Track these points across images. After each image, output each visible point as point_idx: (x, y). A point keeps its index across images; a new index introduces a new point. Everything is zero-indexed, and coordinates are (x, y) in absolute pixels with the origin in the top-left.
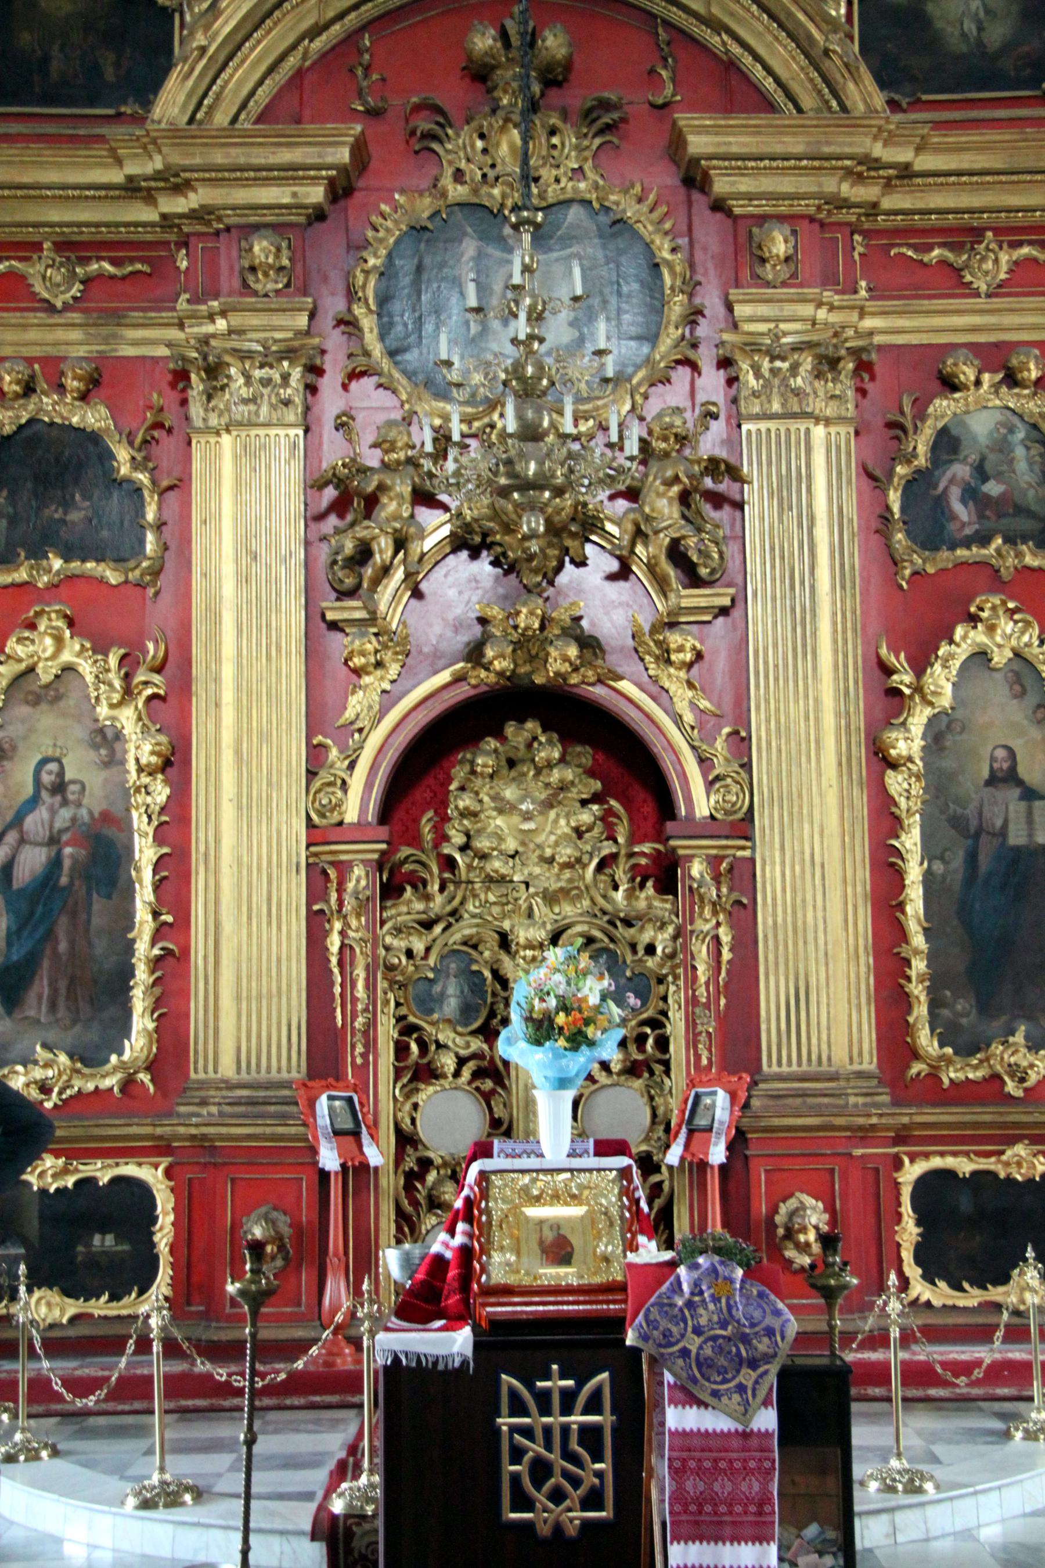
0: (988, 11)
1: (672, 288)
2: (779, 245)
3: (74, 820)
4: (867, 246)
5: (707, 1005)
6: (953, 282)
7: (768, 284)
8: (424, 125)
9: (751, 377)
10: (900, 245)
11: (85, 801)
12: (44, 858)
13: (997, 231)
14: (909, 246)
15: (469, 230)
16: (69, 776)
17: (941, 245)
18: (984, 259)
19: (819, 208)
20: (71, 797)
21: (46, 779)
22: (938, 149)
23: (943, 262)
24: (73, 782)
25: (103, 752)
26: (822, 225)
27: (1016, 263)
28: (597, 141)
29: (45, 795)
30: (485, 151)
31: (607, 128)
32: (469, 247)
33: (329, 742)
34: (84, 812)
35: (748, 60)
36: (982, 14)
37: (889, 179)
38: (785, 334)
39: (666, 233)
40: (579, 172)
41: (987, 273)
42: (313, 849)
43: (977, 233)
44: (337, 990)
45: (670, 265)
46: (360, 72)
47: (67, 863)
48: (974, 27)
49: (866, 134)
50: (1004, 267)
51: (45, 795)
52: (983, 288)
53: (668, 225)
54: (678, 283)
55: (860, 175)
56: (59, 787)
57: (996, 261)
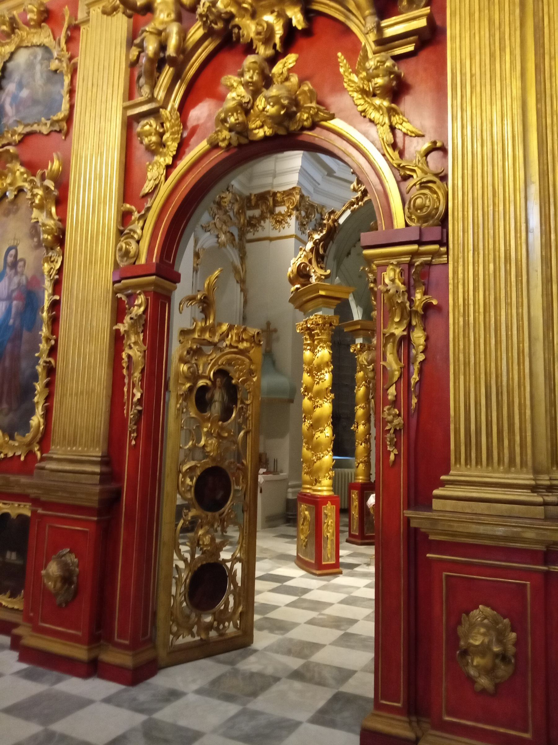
3: (19, 283)
5: (395, 403)
11: (25, 273)
12: (4, 308)
16: (19, 257)
20: (19, 269)
21: (10, 259)
24: (22, 260)
25: (35, 240)
29: (8, 270)
33: (133, 208)
34: (24, 278)
42: (116, 285)
44: (125, 389)
47: (14, 310)
51: (8, 270)
56: (14, 265)
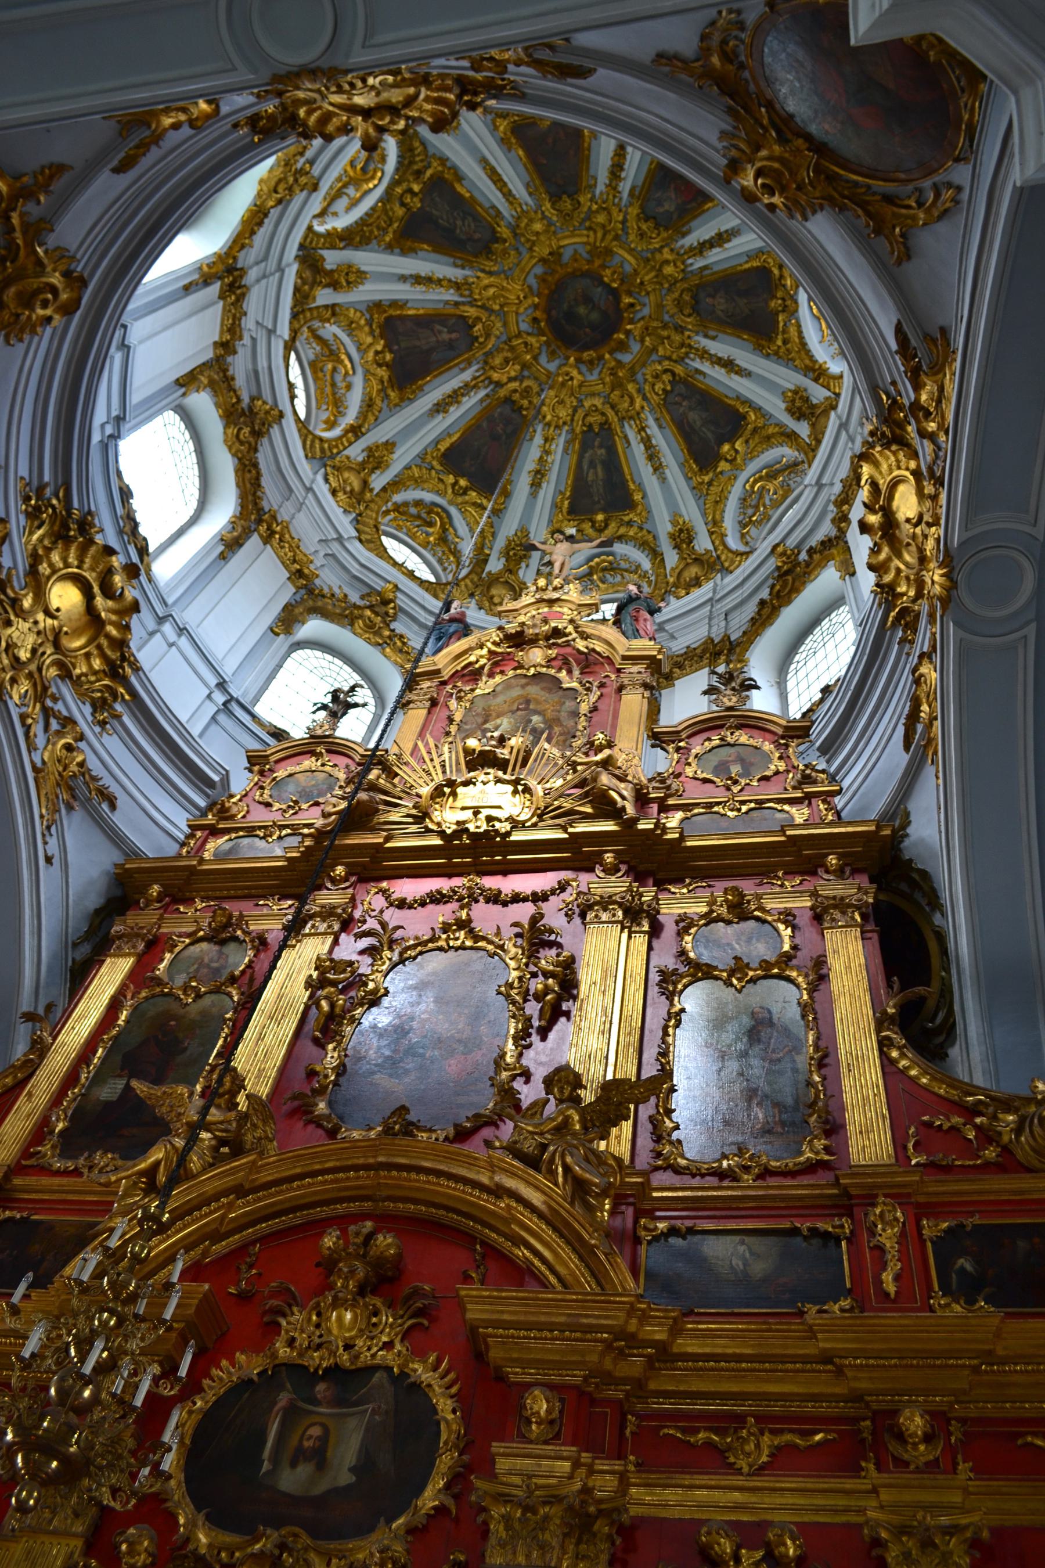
0: (752, 1254)
1: (446, 1443)
2: (540, 1405)
4: (638, 1426)
6: (715, 1460)
7: (531, 1442)
8: (274, 1302)
9: (501, 1528)
10: (668, 1427)
13: (760, 1419)
14: (677, 1428)
15: (288, 1385)
17: (706, 1429)
18: (745, 1441)
19: (586, 1378)
22: (697, 1334)
23: (709, 1444)
26: (593, 1402)
27: (778, 1448)
28: (410, 1322)
30: (318, 1326)
31: (420, 1313)
32: (284, 1399)
35: (537, 1262)
36: (747, 1255)
37: (649, 1356)
38: (538, 1487)
39: (452, 1397)
40: (388, 1346)
41: (748, 1455)
43: (740, 1419)
45: (447, 1421)
46: (244, 1267)
48: (740, 1263)
49: (620, 1310)
50: (766, 1452)
52: (746, 1470)
53: (454, 1390)
54: (453, 1436)
55: (621, 1351)
57: (758, 1446)
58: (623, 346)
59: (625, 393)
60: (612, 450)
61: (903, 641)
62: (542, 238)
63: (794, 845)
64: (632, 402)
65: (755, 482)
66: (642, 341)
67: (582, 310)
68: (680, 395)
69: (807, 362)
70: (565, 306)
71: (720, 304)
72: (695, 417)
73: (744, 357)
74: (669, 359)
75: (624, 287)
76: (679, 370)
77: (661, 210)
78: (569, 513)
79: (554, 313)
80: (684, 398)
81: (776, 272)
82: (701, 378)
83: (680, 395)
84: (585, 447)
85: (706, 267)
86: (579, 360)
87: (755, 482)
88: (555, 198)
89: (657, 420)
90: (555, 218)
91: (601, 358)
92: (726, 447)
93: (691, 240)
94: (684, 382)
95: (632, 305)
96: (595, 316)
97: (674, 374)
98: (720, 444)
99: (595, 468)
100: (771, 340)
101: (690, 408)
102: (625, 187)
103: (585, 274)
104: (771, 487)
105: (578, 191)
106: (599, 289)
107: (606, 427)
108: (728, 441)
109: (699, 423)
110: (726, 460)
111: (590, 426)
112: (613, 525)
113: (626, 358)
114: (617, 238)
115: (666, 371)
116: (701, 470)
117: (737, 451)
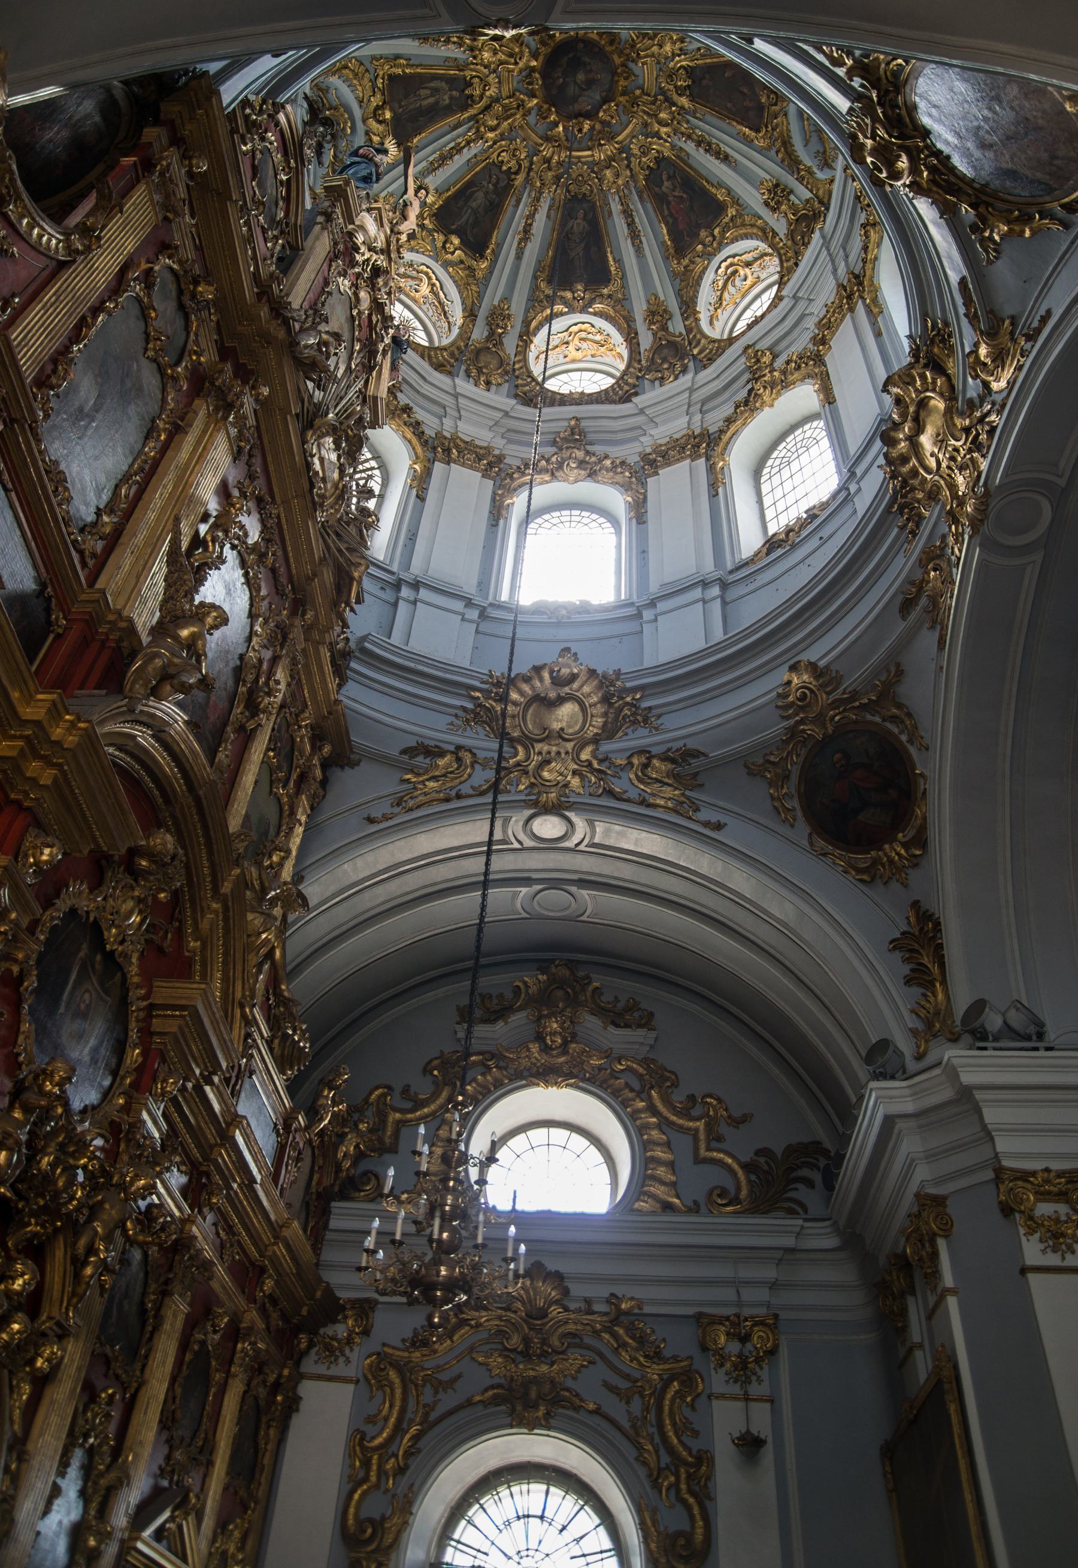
58: (543, 116)
59: (501, 119)
60: (449, 110)
61: (464, 709)
62: (655, 49)
63: (330, 713)
64: (492, 129)
65: (427, 274)
66: (547, 139)
67: (581, 77)
68: (498, 182)
69: (534, 324)
70: (587, 59)
71: (579, 225)
72: (479, 200)
73: (532, 250)
74: (530, 169)
75: (598, 126)
76: (520, 179)
77: (664, 177)
78: (390, 76)
79: (581, 45)
80: (495, 185)
81: (605, 291)
82: (513, 202)
83: (498, 179)
84: (451, 81)
85: (610, 213)
86: (533, 70)
87: (427, 274)
88: (690, 71)
89: (476, 156)
90: (672, 64)
91: (532, 95)
92: (456, 241)
93: (636, 205)
94: (509, 186)
95: (580, 131)
96: (571, 90)
97: (517, 173)
98: (458, 233)
99: (432, 95)
100: (549, 282)
101: (486, 193)
102: (690, 147)
103: (613, 83)
104: (425, 289)
105: (692, 98)
106: (598, 97)
107: (467, 102)
108: (462, 242)
109: (474, 205)
110: (445, 243)
111: (470, 84)
112: (381, 128)
113: (532, 119)
114: (646, 125)
115: (520, 166)
116: (434, 215)
117: (453, 253)
